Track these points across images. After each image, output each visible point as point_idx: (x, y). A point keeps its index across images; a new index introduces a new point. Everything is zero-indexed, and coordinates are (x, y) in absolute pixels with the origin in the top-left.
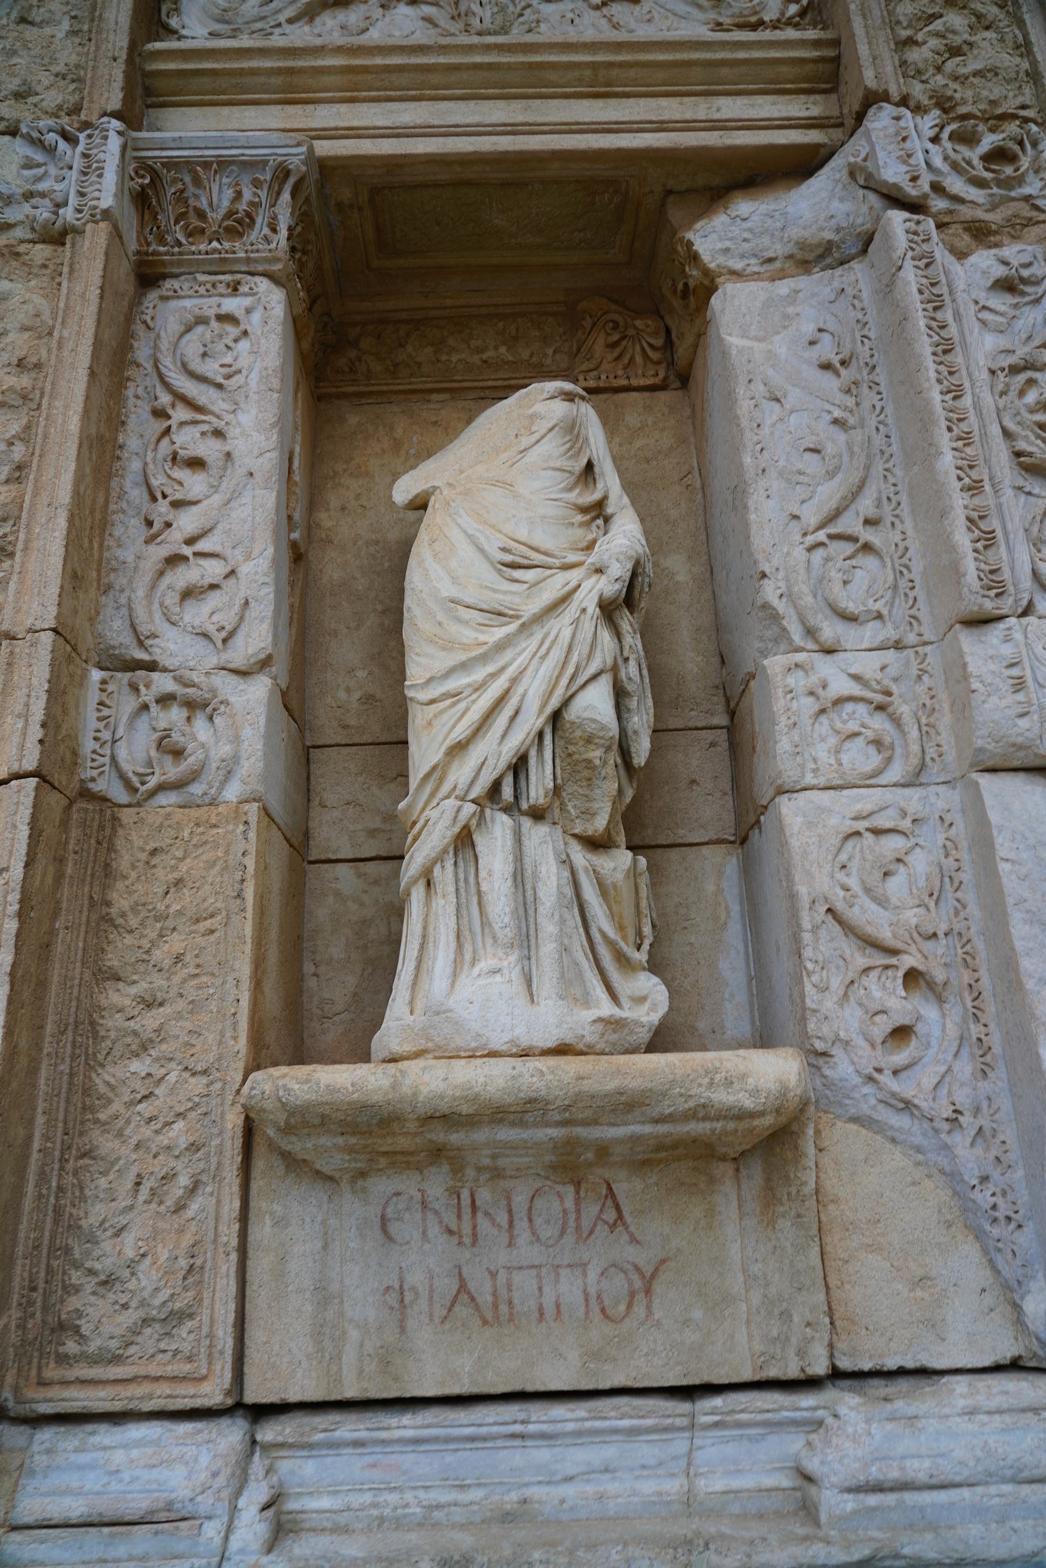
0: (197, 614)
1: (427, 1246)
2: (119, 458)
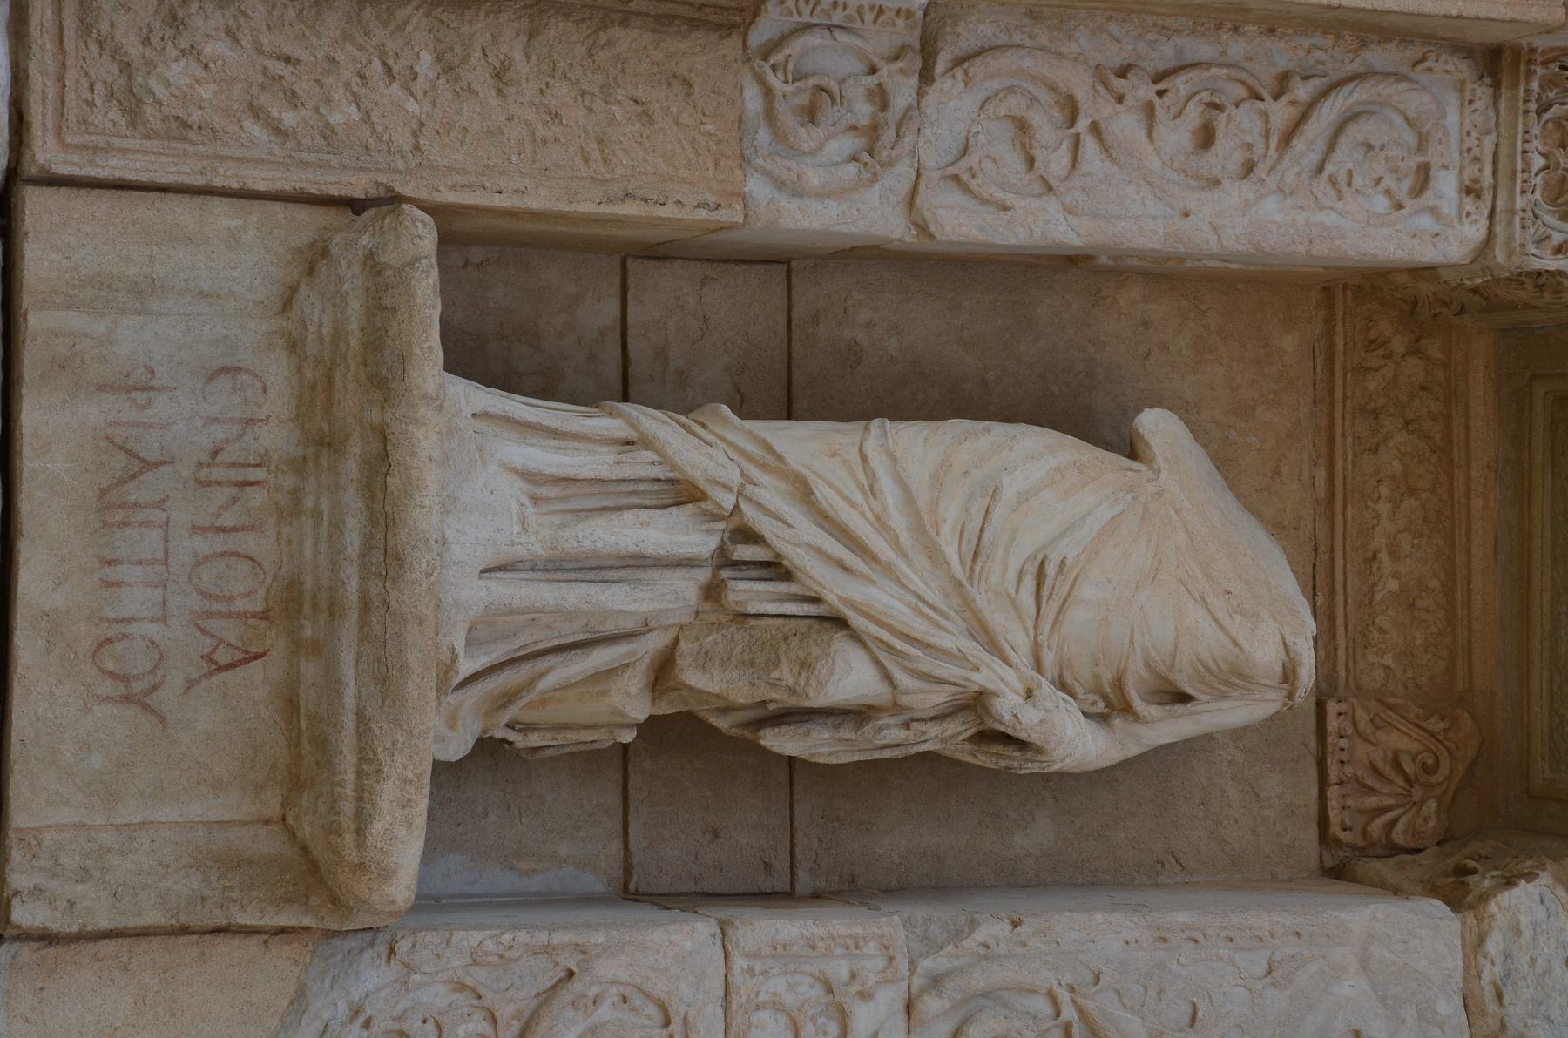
1: (199, 423)
2: (1219, 27)
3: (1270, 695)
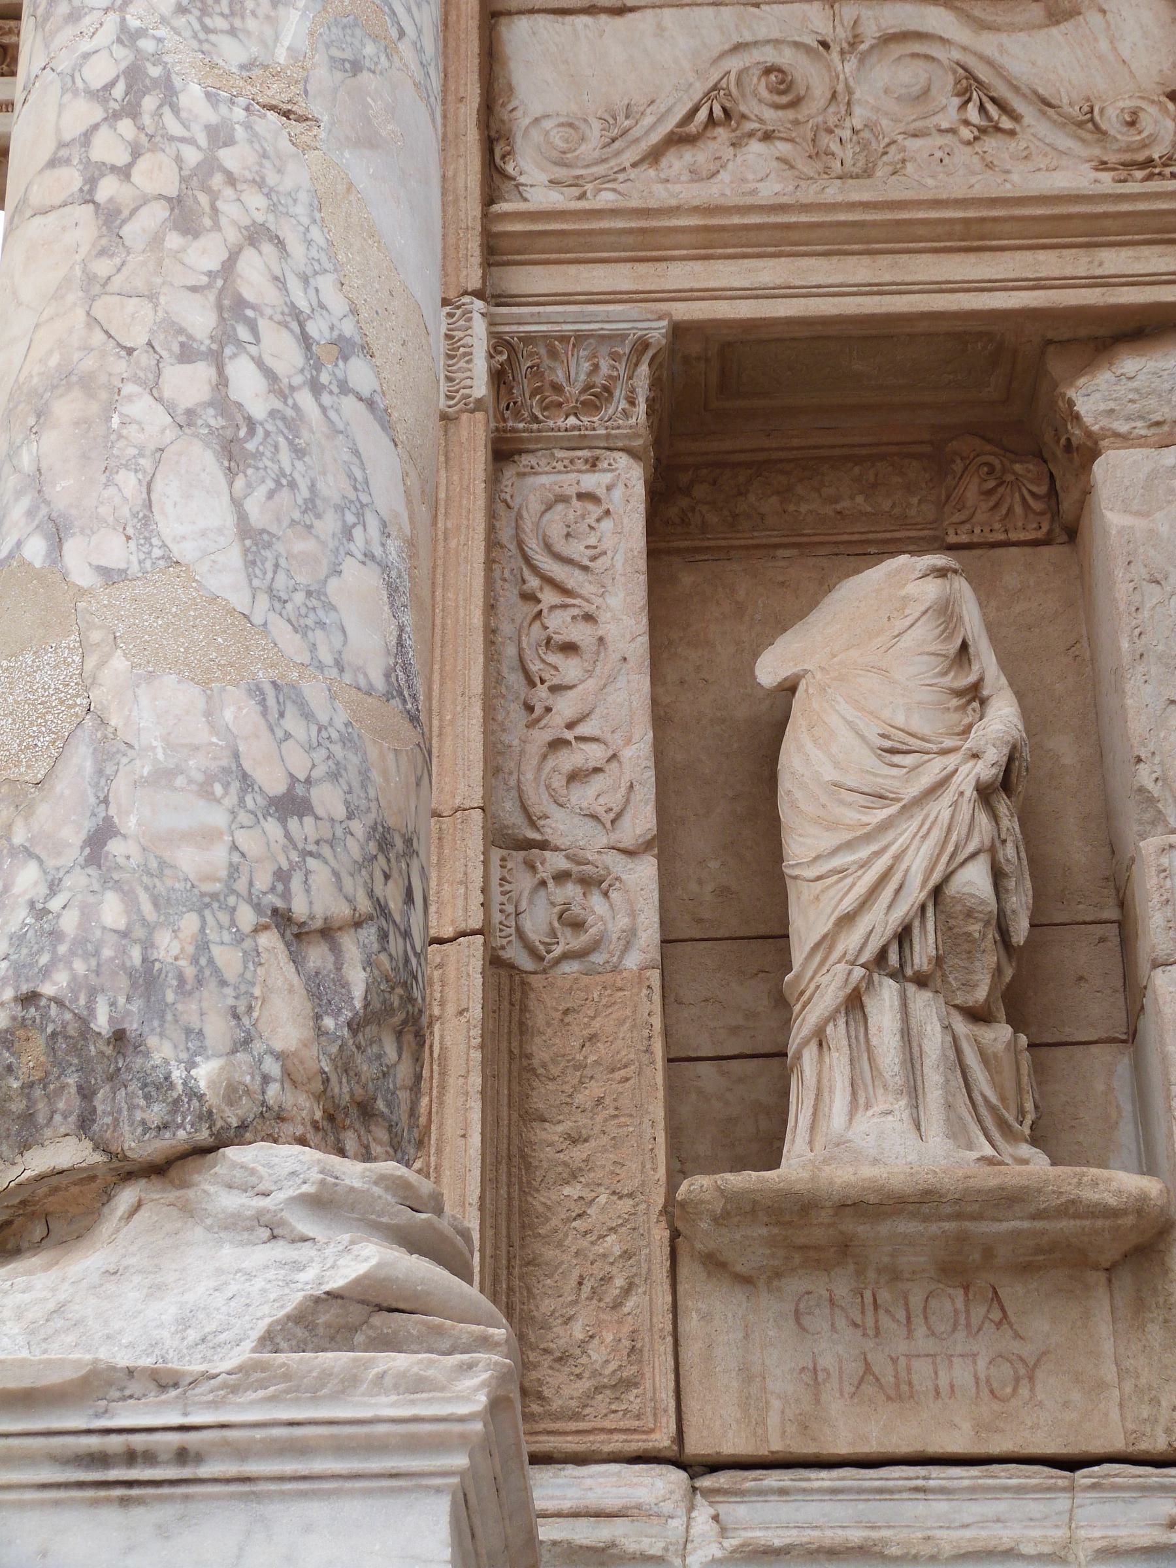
0: (585, 795)
1: (835, 1336)
3: (956, 585)
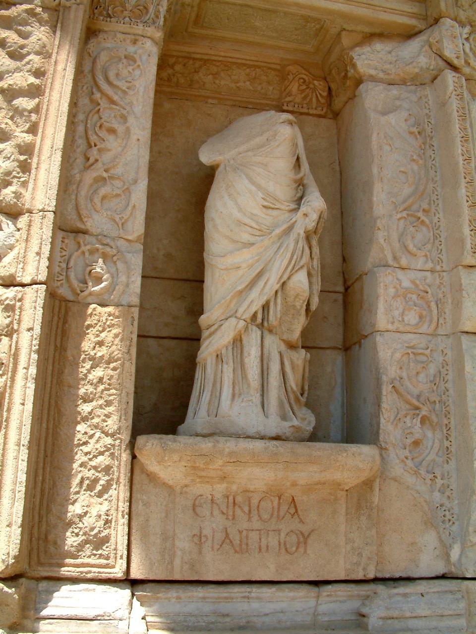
1: (213, 519)
